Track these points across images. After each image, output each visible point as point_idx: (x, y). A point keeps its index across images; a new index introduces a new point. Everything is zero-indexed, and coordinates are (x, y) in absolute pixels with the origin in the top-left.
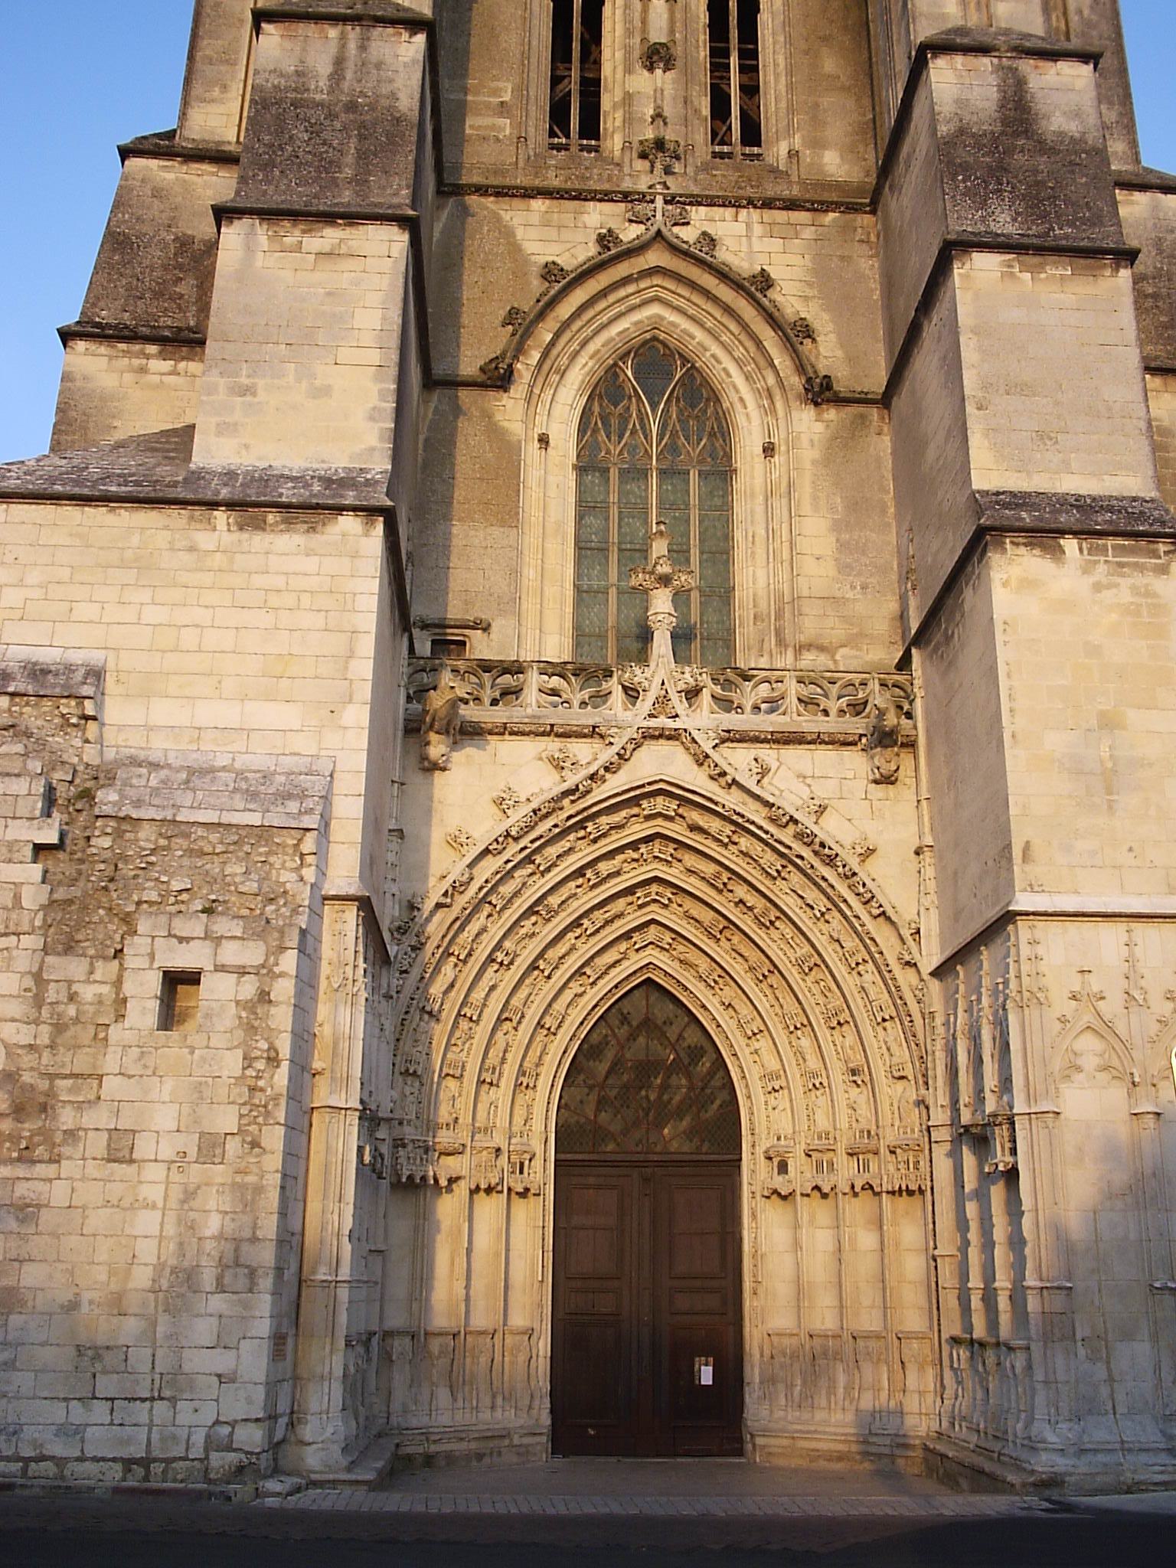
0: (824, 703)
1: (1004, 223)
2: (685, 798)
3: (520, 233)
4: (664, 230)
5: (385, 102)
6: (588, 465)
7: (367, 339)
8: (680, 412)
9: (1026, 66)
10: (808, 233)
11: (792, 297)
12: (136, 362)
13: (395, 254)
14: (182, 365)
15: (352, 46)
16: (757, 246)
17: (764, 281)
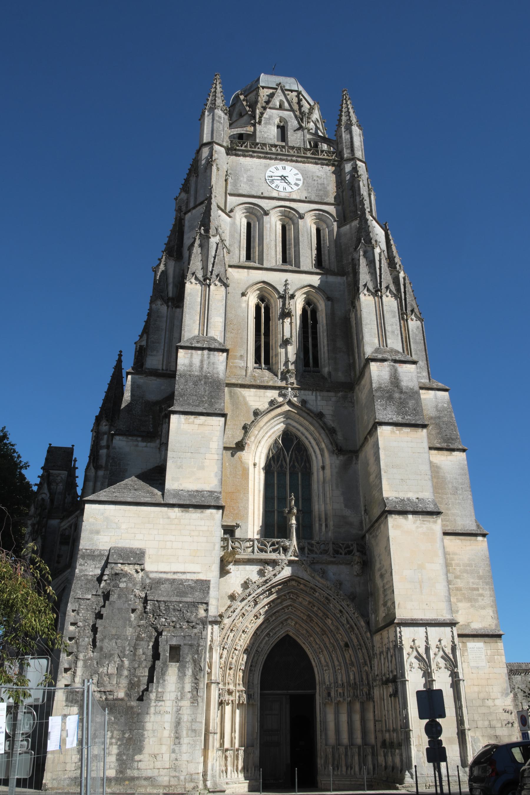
0: (341, 551)
3: (248, 399)
4: (291, 399)
5: (216, 376)
7: (214, 451)
8: (296, 454)
9: (397, 365)
10: (334, 399)
11: (329, 420)
12: (135, 443)
13: (221, 425)
14: (149, 444)
15: (206, 356)
16: (319, 403)
17: (320, 416)
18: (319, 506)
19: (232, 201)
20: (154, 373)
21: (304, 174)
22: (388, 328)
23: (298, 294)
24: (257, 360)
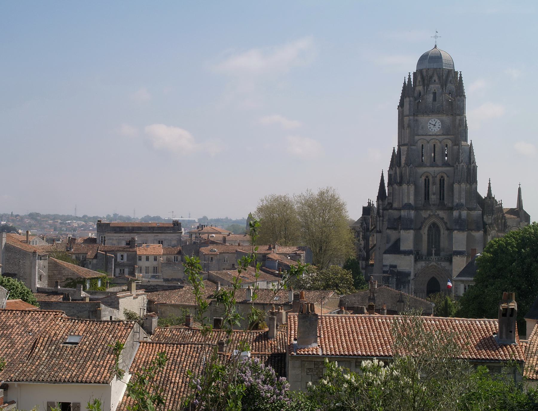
1: (457, 228)
2: (435, 266)
6: (428, 235)
11: (445, 220)
17: (443, 219)
18: (442, 245)
19: (417, 138)
20: (396, 209)
21: (442, 122)
22: (462, 196)
23: (438, 176)
24: (425, 199)
